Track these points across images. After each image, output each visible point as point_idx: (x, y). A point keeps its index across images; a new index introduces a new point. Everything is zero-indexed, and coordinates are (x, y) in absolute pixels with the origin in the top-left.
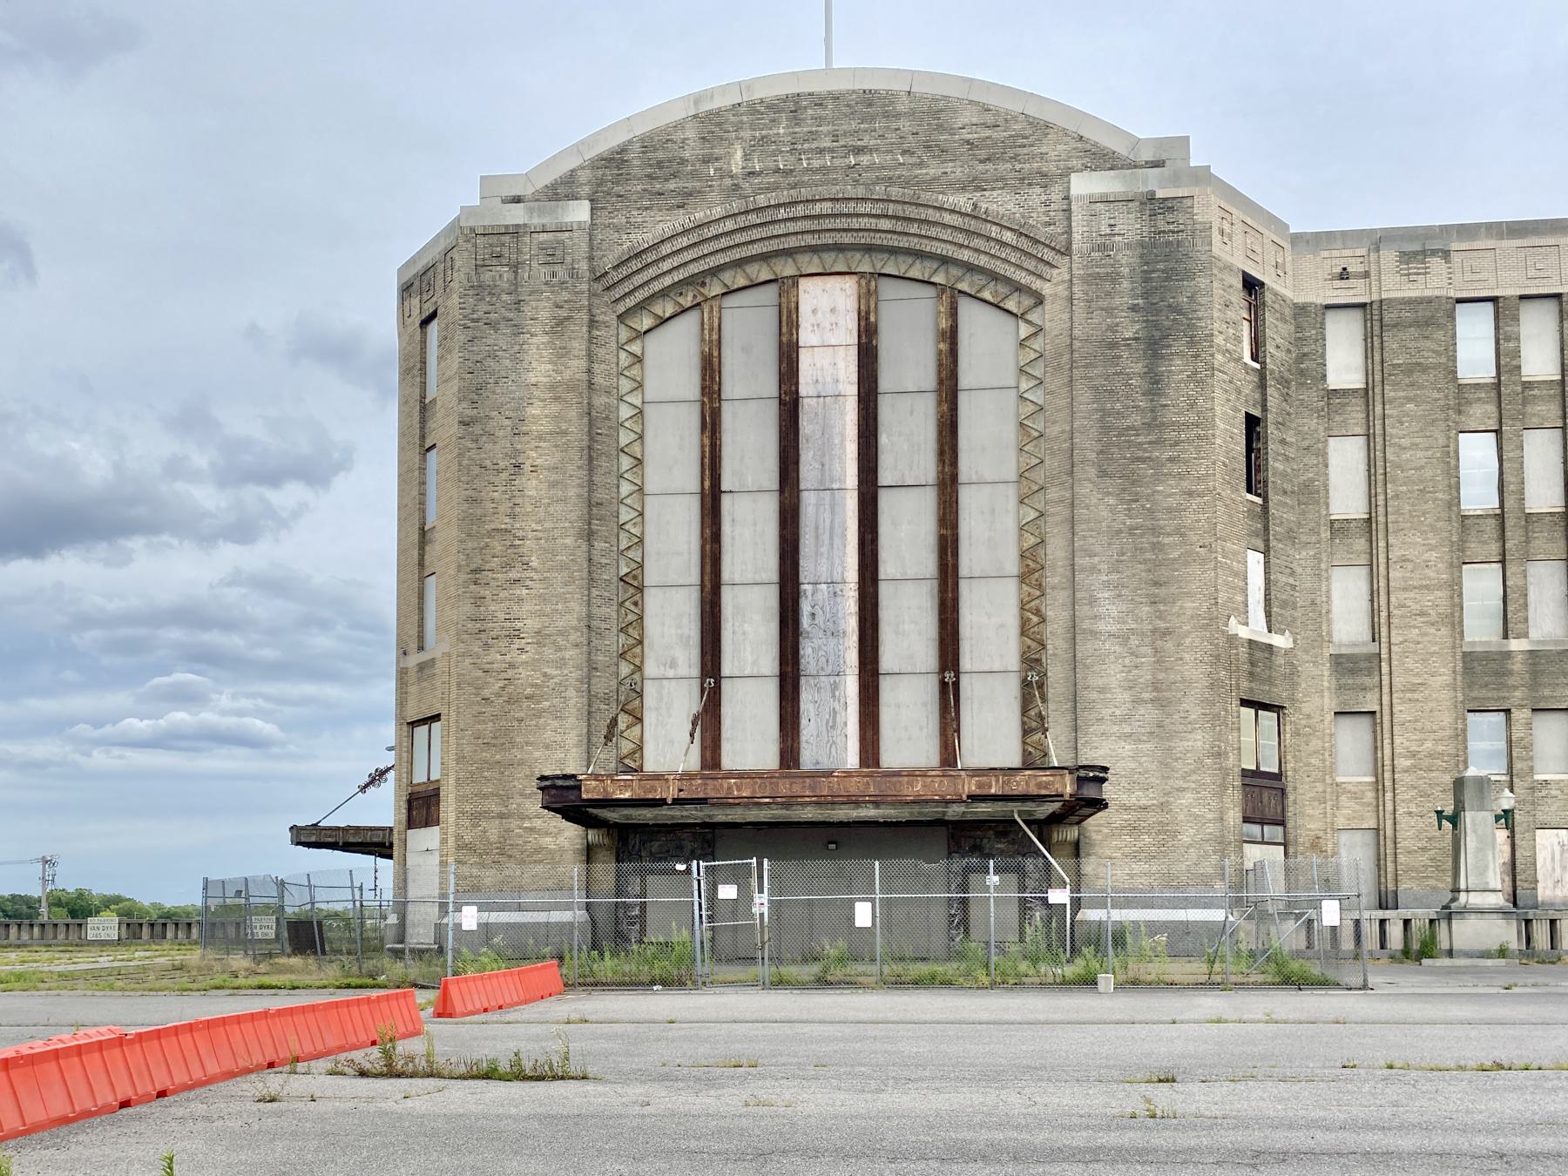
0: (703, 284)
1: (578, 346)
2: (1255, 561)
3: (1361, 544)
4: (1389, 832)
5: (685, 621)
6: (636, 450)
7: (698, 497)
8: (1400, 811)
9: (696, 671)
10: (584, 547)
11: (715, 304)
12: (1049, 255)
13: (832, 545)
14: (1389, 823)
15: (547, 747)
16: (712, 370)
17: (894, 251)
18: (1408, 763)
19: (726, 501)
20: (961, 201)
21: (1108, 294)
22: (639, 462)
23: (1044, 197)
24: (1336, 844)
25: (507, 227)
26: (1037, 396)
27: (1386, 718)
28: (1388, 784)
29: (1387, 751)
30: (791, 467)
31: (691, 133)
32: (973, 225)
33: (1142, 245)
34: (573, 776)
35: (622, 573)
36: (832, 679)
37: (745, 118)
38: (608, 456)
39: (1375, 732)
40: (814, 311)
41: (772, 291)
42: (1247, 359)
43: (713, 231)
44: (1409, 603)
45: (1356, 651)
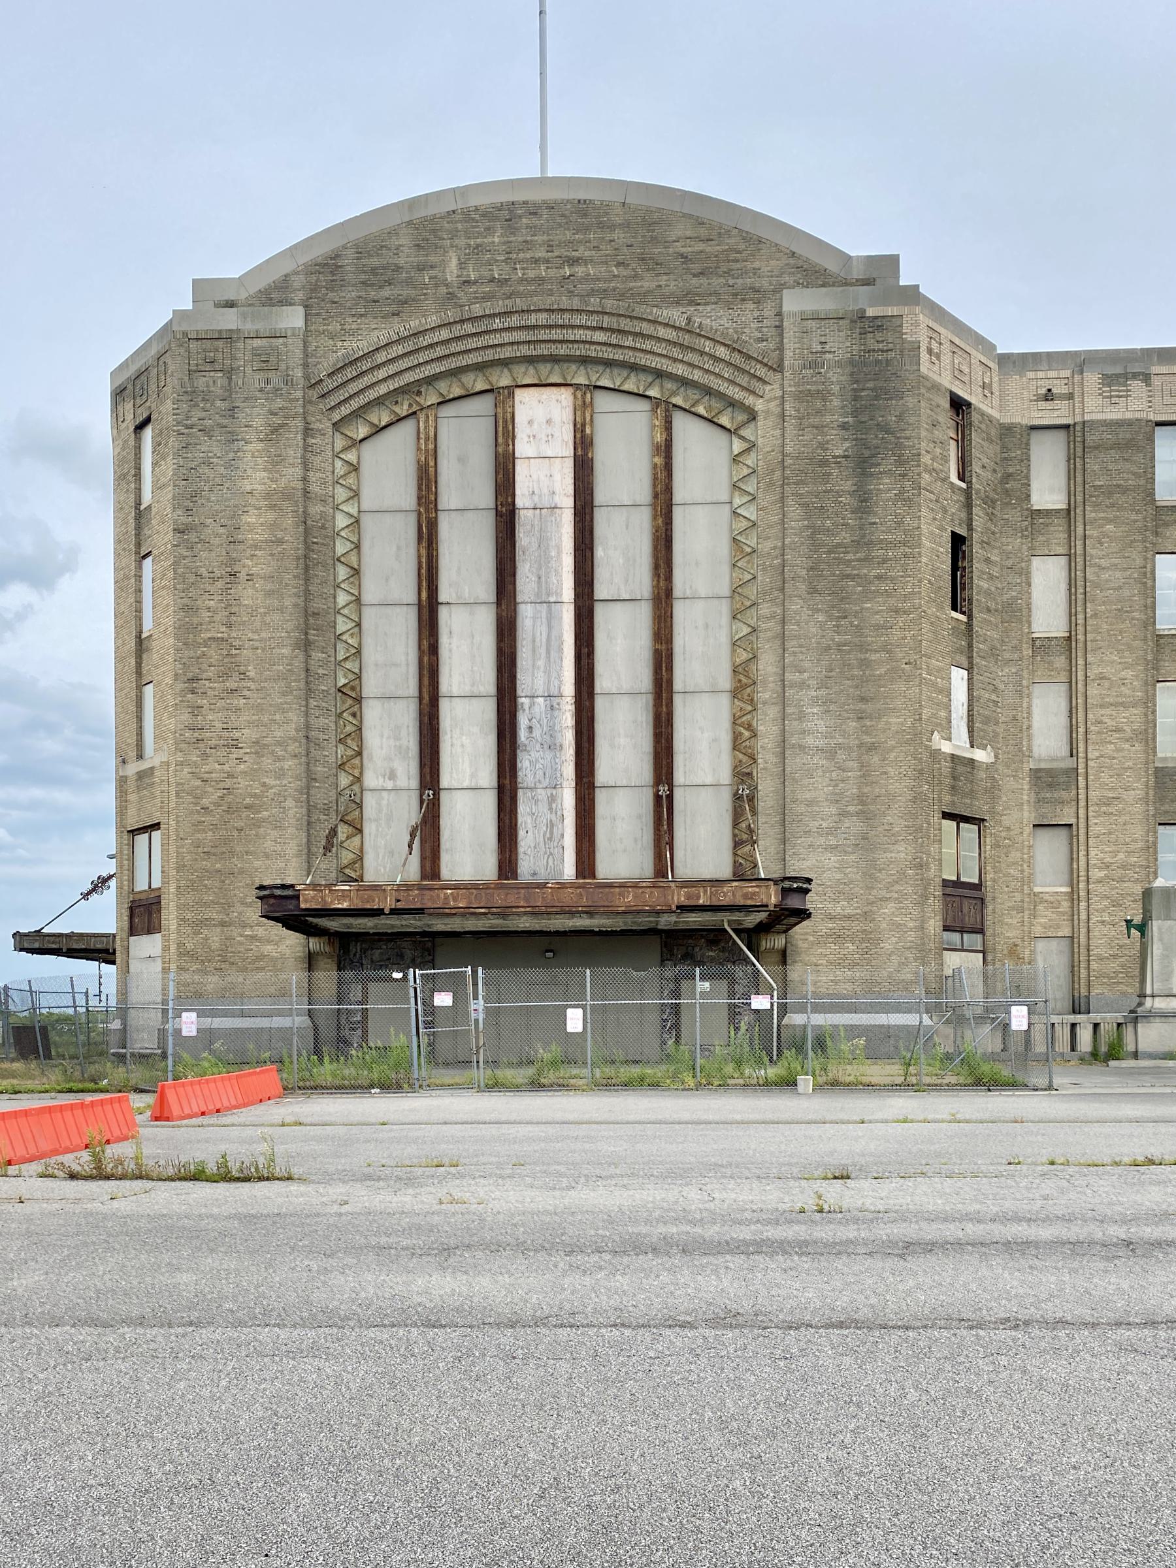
0: (419, 393)
1: (293, 454)
2: (959, 678)
3: (1060, 662)
4: (1083, 940)
5: (404, 732)
6: (353, 559)
7: (416, 609)
8: (1094, 919)
9: (414, 783)
10: (301, 657)
11: (431, 413)
12: (761, 371)
13: (548, 658)
14: (1083, 931)
15: (267, 856)
16: (428, 480)
17: (609, 363)
18: (1102, 874)
19: (443, 613)
20: (676, 315)
21: (819, 412)
22: (356, 572)
23: (756, 314)
24: (1033, 952)
25: (220, 331)
26: (750, 512)
27: (1082, 831)
28: (1082, 893)
29: (1082, 863)
30: (508, 579)
31: (405, 240)
32: (687, 339)
33: (851, 362)
34: (292, 886)
36: (549, 792)
37: (459, 226)
39: (1071, 844)
40: (530, 422)
41: (488, 400)
42: (954, 478)
44: (1105, 719)
45: (1054, 765)
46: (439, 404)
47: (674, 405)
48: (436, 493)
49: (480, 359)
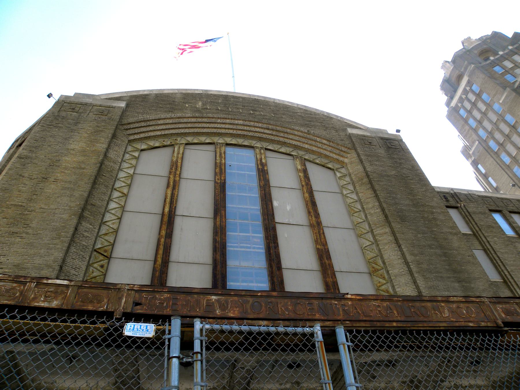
16: (177, 166)
38: (107, 186)
43: (185, 120)
46: (186, 144)
47: (305, 159)
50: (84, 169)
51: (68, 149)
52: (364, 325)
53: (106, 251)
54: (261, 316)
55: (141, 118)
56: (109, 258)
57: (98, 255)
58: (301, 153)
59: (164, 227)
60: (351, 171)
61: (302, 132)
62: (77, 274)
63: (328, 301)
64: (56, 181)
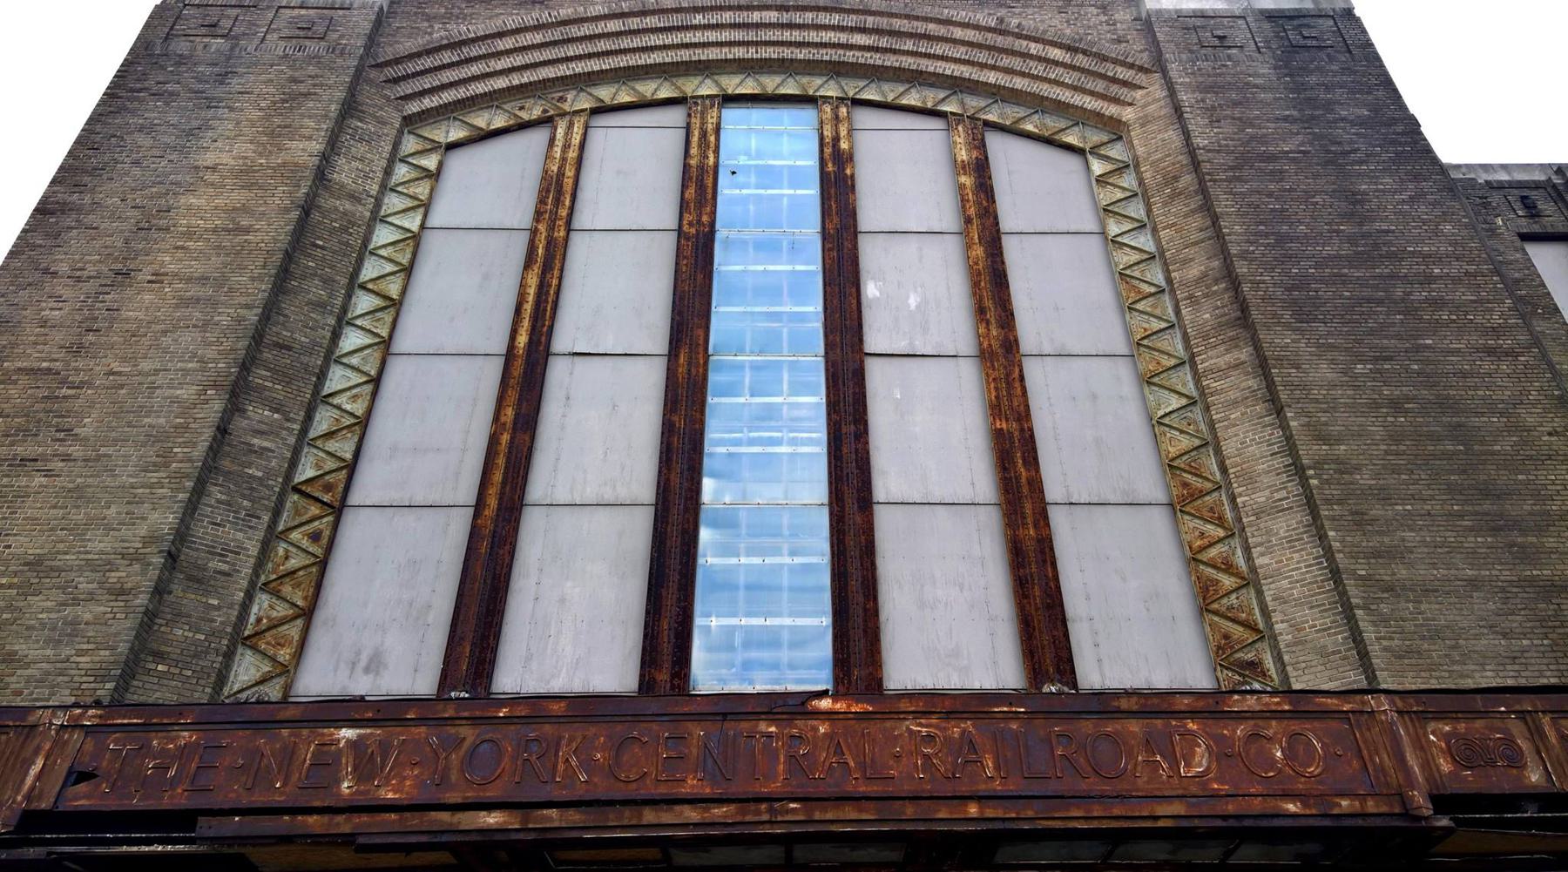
12: (1123, 73)
32: (1000, 41)
35: (299, 478)
38: (328, 282)
41: (676, 116)
43: (586, 29)
46: (595, 112)
47: (987, 124)
48: (572, 208)
49: (668, 60)
50: (247, 231)
51: (197, 168)
52: (854, 816)
53: (328, 488)
54: (491, 794)
55: (439, 34)
56: (338, 510)
57: (303, 502)
58: (973, 103)
59: (512, 395)
60: (1140, 151)
61: (977, 27)
62: (225, 567)
63: (744, 725)
64: (158, 278)
